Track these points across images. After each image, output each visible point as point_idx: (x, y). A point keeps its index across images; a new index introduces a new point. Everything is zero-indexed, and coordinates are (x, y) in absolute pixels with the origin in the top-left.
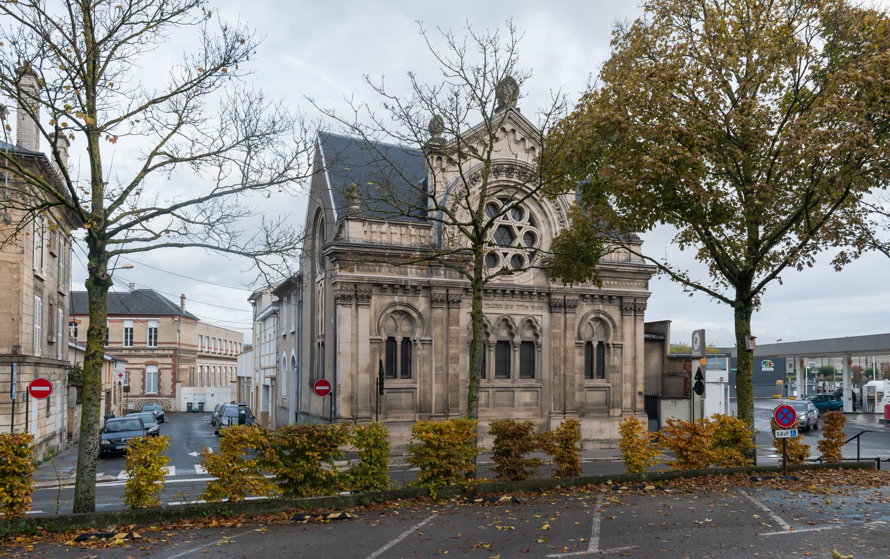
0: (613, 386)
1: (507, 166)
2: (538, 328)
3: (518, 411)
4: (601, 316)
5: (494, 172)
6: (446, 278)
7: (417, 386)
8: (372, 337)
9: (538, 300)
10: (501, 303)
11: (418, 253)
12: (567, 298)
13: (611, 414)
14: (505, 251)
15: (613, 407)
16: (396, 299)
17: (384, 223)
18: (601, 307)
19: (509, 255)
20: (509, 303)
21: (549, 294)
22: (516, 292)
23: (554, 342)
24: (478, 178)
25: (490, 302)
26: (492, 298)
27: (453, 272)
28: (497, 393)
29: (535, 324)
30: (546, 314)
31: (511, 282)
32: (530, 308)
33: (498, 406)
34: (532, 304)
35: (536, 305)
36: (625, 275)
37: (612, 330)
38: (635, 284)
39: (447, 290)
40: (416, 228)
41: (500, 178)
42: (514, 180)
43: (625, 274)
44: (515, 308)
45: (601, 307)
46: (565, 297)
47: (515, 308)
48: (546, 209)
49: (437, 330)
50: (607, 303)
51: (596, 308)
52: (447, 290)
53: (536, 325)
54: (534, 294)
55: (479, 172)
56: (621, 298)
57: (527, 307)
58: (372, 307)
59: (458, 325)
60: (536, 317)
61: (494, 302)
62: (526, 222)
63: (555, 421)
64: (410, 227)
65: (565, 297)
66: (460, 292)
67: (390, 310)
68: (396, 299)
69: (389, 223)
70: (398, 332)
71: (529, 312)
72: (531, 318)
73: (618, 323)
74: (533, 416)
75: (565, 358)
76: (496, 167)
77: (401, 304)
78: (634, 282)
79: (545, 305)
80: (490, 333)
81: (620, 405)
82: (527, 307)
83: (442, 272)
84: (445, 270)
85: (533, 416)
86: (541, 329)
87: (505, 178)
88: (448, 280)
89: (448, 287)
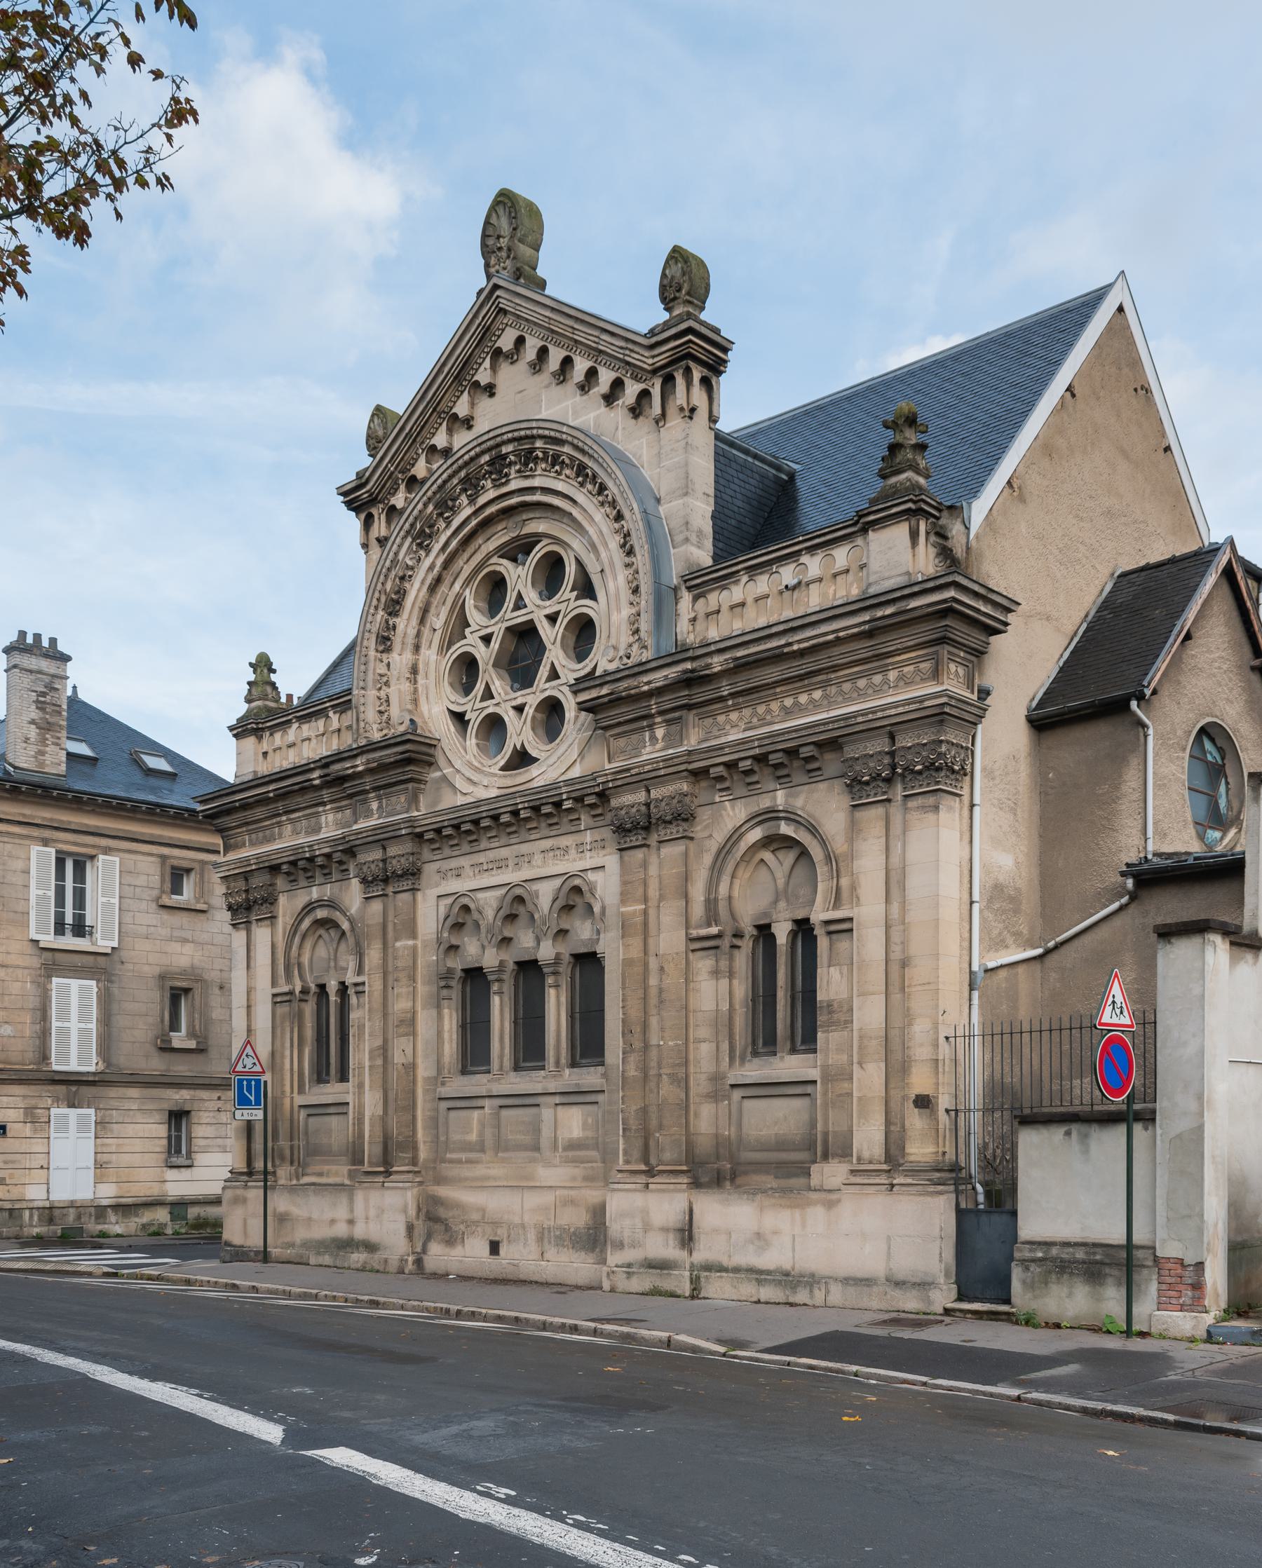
0: (828, 1077)
3: (548, 1164)
4: (785, 829)
7: (349, 1098)
8: (276, 991)
9: (591, 822)
12: (653, 794)
13: (815, 1181)
15: (826, 1157)
16: (315, 893)
18: (780, 798)
20: (524, 848)
21: (603, 796)
23: (626, 946)
25: (481, 858)
26: (484, 844)
27: (394, 799)
28: (504, 1112)
30: (611, 860)
32: (573, 852)
33: (506, 1150)
36: (837, 655)
37: (821, 870)
38: (892, 675)
43: (836, 651)
45: (780, 798)
47: (538, 859)
49: (373, 956)
50: (799, 777)
51: (765, 802)
54: (567, 805)
56: (833, 745)
57: (566, 850)
58: (280, 920)
59: (414, 935)
61: (491, 855)
63: (617, 1196)
66: (408, 847)
67: (306, 923)
68: (315, 893)
70: (332, 972)
71: (571, 864)
73: (839, 845)
74: (586, 1178)
75: (661, 991)
77: (320, 904)
78: (884, 670)
79: (607, 833)
81: (845, 1152)
82: (566, 850)
83: (375, 805)
84: (379, 798)
85: (586, 1178)
89: (382, 838)
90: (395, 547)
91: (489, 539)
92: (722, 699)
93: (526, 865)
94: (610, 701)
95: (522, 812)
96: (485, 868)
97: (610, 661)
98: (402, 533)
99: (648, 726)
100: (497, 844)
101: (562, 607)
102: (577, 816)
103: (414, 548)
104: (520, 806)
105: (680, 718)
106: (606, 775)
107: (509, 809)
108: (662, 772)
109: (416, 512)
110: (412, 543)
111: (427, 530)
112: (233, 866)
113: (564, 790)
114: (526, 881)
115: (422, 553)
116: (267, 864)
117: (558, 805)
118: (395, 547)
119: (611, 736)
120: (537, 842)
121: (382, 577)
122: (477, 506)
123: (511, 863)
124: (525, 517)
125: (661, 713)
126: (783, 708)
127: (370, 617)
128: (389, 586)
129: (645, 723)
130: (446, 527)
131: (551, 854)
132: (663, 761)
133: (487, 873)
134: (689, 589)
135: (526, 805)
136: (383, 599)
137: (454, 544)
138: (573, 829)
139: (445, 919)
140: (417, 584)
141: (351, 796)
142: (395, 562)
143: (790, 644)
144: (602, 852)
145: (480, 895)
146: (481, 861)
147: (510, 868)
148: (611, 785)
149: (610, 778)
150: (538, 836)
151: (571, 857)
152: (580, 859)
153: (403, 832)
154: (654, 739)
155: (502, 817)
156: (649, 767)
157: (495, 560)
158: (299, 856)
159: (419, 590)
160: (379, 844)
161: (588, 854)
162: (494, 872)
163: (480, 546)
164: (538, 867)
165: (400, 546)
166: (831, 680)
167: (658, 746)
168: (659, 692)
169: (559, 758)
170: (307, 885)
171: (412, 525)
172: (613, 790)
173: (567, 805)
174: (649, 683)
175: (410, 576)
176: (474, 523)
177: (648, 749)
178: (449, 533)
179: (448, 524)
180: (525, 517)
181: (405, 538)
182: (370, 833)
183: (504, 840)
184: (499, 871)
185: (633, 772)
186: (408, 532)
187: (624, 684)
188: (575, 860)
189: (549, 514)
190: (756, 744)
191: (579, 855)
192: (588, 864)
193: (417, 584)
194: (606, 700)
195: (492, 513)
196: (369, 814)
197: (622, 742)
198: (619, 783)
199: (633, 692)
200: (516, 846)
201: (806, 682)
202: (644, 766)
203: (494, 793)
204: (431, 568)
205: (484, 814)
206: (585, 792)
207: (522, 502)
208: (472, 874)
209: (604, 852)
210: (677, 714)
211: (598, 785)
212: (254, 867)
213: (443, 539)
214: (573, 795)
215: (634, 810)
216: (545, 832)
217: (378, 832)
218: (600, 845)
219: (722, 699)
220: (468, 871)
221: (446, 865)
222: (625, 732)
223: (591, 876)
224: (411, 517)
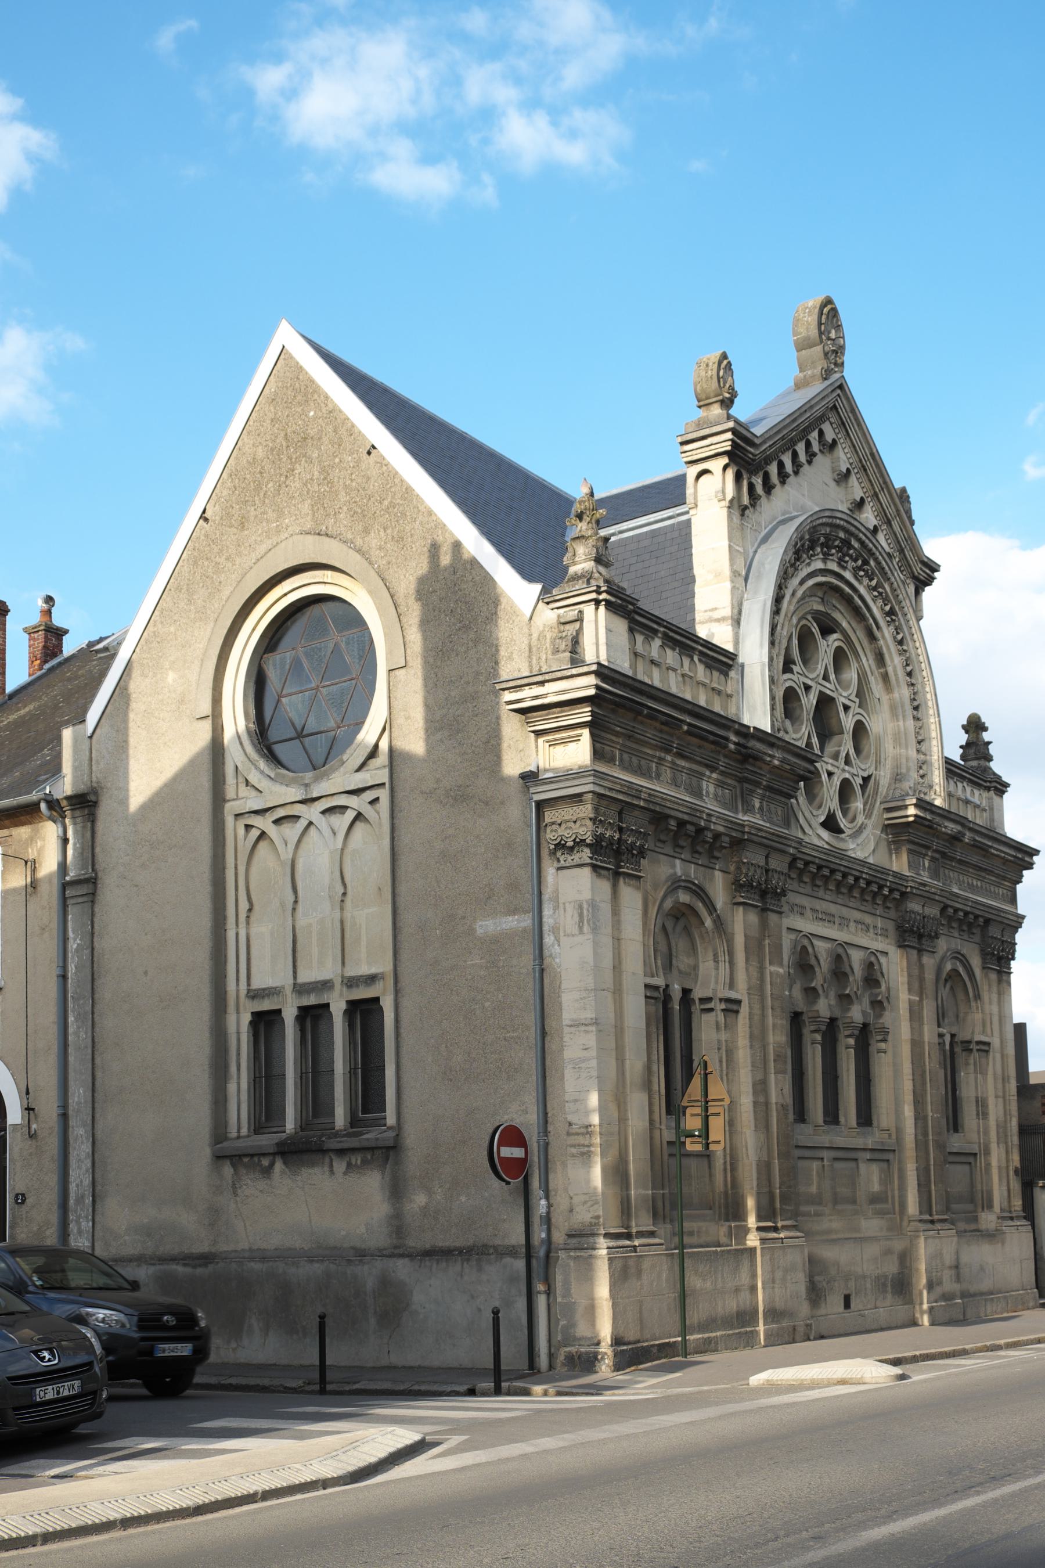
11: (733, 738)
17: (655, 632)
26: (821, 893)
40: (708, 666)
48: (890, 669)
56: (987, 921)
62: (853, 697)
64: (696, 658)
69: (666, 636)
92: (952, 859)
108: (937, 898)
112: (618, 787)
113: (890, 878)
116: (658, 809)
120: (852, 911)
126: (968, 883)
129: (924, 852)
131: (860, 926)
138: (873, 911)
143: (991, 847)
145: (816, 942)
158: (695, 820)
166: (985, 878)
170: (672, 853)
184: (830, 925)
185: (927, 888)
190: (970, 904)
198: (918, 892)
201: (979, 873)
209: (887, 941)
211: (906, 887)
212: (642, 803)
217: (774, 838)
218: (884, 933)
219: (952, 859)
220: (808, 913)
223: (883, 960)
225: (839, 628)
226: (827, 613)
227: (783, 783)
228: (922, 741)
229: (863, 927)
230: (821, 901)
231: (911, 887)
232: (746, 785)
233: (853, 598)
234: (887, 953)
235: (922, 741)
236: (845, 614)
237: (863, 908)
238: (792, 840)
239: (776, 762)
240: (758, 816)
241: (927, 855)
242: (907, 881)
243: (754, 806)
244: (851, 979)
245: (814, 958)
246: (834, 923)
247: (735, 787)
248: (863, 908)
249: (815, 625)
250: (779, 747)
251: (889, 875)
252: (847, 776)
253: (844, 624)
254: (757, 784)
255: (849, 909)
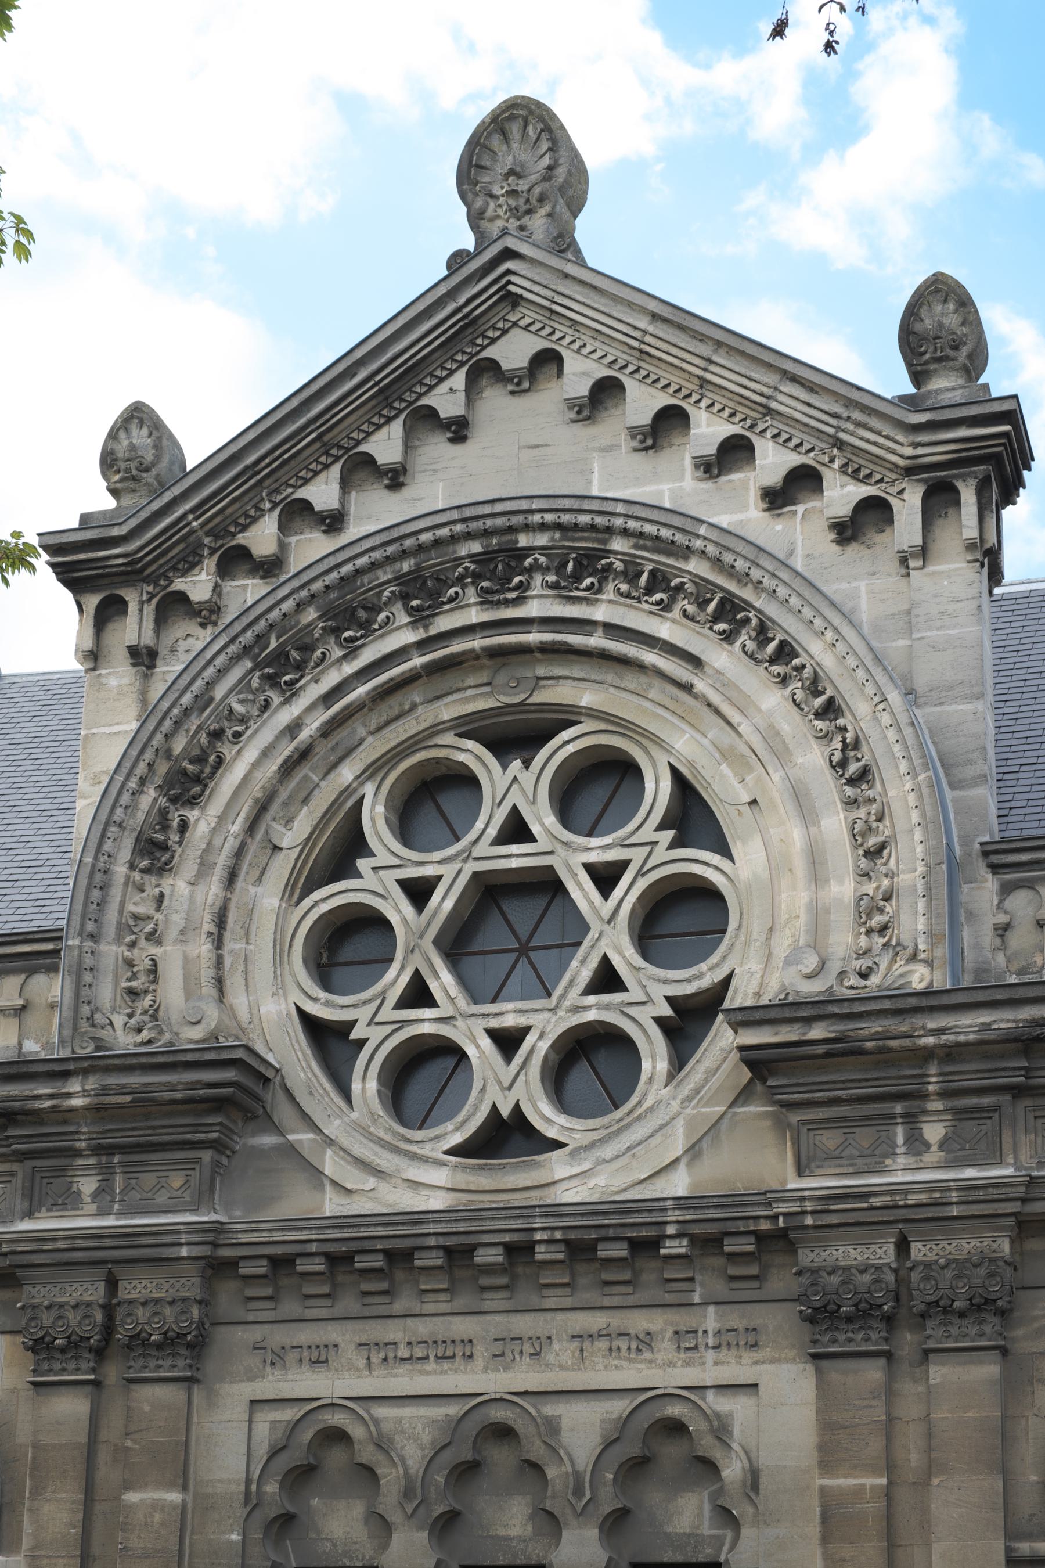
1: (476, 547)
2: (732, 1471)
5: (405, 597)
6: (101, 1213)
9: (720, 1288)
10: (462, 1327)
12: (918, 1251)
14: (510, 1021)
19: (530, 1039)
20: (523, 1324)
22: (542, 1253)
24: (306, 648)
25: (394, 1331)
27: (149, 1179)
29: (707, 1446)
31: (533, 1198)
32: (665, 1348)
34: (683, 1319)
35: (711, 1320)
39: (112, 1284)
41: (444, 623)
42: (533, 609)
44: (562, 1351)
46: (903, 1246)
47: (562, 1351)
52: (112, 1284)
53: (717, 1454)
54: (672, 1248)
55: (311, 614)
60: (714, 1402)
61: (423, 1328)
62: (647, 833)
65: (903, 1246)
72: (675, 1410)
76: (406, 566)
80: (395, 1517)
83: (88, 1185)
84: (106, 1172)
86: (753, 1479)
87: (474, 616)
88: (110, 1221)
90: (211, 671)
91: (438, 698)
93: (527, 1359)
94: (828, 1055)
95: (540, 1249)
96: (403, 1352)
97: (809, 977)
98: (233, 649)
99: (903, 1115)
100: (443, 1307)
101: (637, 856)
102: (690, 1275)
103: (255, 683)
104: (538, 1236)
105: (996, 1108)
106: (803, 1199)
107: (507, 1238)
109: (275, 615)
110: (252, 671)
111: (295, 654)
114: (526, 1393)
115: (276, 699)
117: (654, 1245)
118: (211, 671)
119: (803, 1122)
120: (560, 1316)
121: (168, 724)
122: (433, 631)
123: (479, 1350)
124: (541, 671)
125: (944, 1094)
127: (125, 798)
128: (179, 745)
130: (345, 657)
131: (603, 1344)
132: (960, 1189)
133: (407, 1366)
134: (995, 868)
135: (558, 1235)
136: (163, 768)
137: (361, 691)
138: (669, 1298)
139: (275, 1453)
140: (251, 754)
141: (22, 1156)
142: (203, 700)
144: (748, 1356)
145: (382, 1411)
146: (390, 1337)
147: (479, 1362)
148: (809, 1221)
149: (809, 1206)
150: (568, 1302)
151: (660, 1357)
152: (687, 1364)
153: (184, 1252)
154: (916, 1144)
155: (480, 1251)
156: (923, 1197)
157: (449, 738)
159: (255, 765)
160: (101, 1272)
161: (710, 1356)
162: (431, 1365)
163: (414, 707)
164: (562, 1367)
165: (221, 672)
167: (929, 1158)
168: (952, 1053)
169: (629, 1149)
171: (261, 639)
172: (812, 1234)
173: (672, 1248)
174: (941, 1031)
175: (237, 735)
176: (418, 661)
177: (901, 1161)
178: (349, 669)
179: (352, 651)
180: (541, 671)
181: (236, 659)
182: (79, 1243)
183: (461, 1302)
184: (446, 1365)
185: (876, 1202)
186: (246, 650)
187: (875, 1027)
188: (671, 1364)
189: (610, 678)
191: (682, 1355)
192: (710, 1375)
193: (251, 754)
194: (820, 1050)
195: (472, 651)
196: (69, 1201)
197: (830, 1139)
198: (835, 1219)
199: (894, 1044)
200: (498, 1318)
202: (906, 1192)
203: (437, 1202)
204: (293, 729)
205: (432, 1241)
206: (731, 1226)
207: (554, 643)
208: (362, 1363)
210: (986, 1101)
211: (776, 1217)
213: (332, 678)
214: (696, 1230)
215: (867, 1278)
216: (591, 1296)
217: (107, 1243)
221: (279, 1336)
222: (844, 1119)
224: (263, 623)
225: (580, 714)
226: (509, 706)
227: (154, 1128)
228: (882, 847)
229: (623, 1344)
230: (409, 1321)
231: (785, 1215)
232: (30, 1164)
233: (565, 643)
234: (757, 1385)
235: (882, 847)
236: (593, 677)
237: (607, 1302)
238: (178, 1232)
239: (77, 1102)
240: (93, 1208)
241: (925, 1112)
242: (769, 1204)
243: (79, 1193)
244: (551, 1472)
245: (371, 1448)
246: (471, 1357)
247: (13, 1174)
248: (607, 1302)
249: (470, 744)
250: (86, 1072)
251: (664, 1210)
252: (591, 1016)
253: (587, 698)
254: (77, 1153)
255: (549, 1316)
